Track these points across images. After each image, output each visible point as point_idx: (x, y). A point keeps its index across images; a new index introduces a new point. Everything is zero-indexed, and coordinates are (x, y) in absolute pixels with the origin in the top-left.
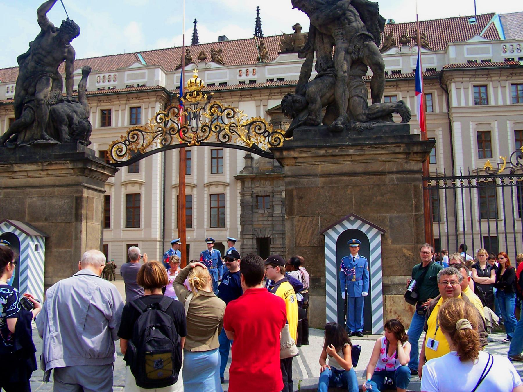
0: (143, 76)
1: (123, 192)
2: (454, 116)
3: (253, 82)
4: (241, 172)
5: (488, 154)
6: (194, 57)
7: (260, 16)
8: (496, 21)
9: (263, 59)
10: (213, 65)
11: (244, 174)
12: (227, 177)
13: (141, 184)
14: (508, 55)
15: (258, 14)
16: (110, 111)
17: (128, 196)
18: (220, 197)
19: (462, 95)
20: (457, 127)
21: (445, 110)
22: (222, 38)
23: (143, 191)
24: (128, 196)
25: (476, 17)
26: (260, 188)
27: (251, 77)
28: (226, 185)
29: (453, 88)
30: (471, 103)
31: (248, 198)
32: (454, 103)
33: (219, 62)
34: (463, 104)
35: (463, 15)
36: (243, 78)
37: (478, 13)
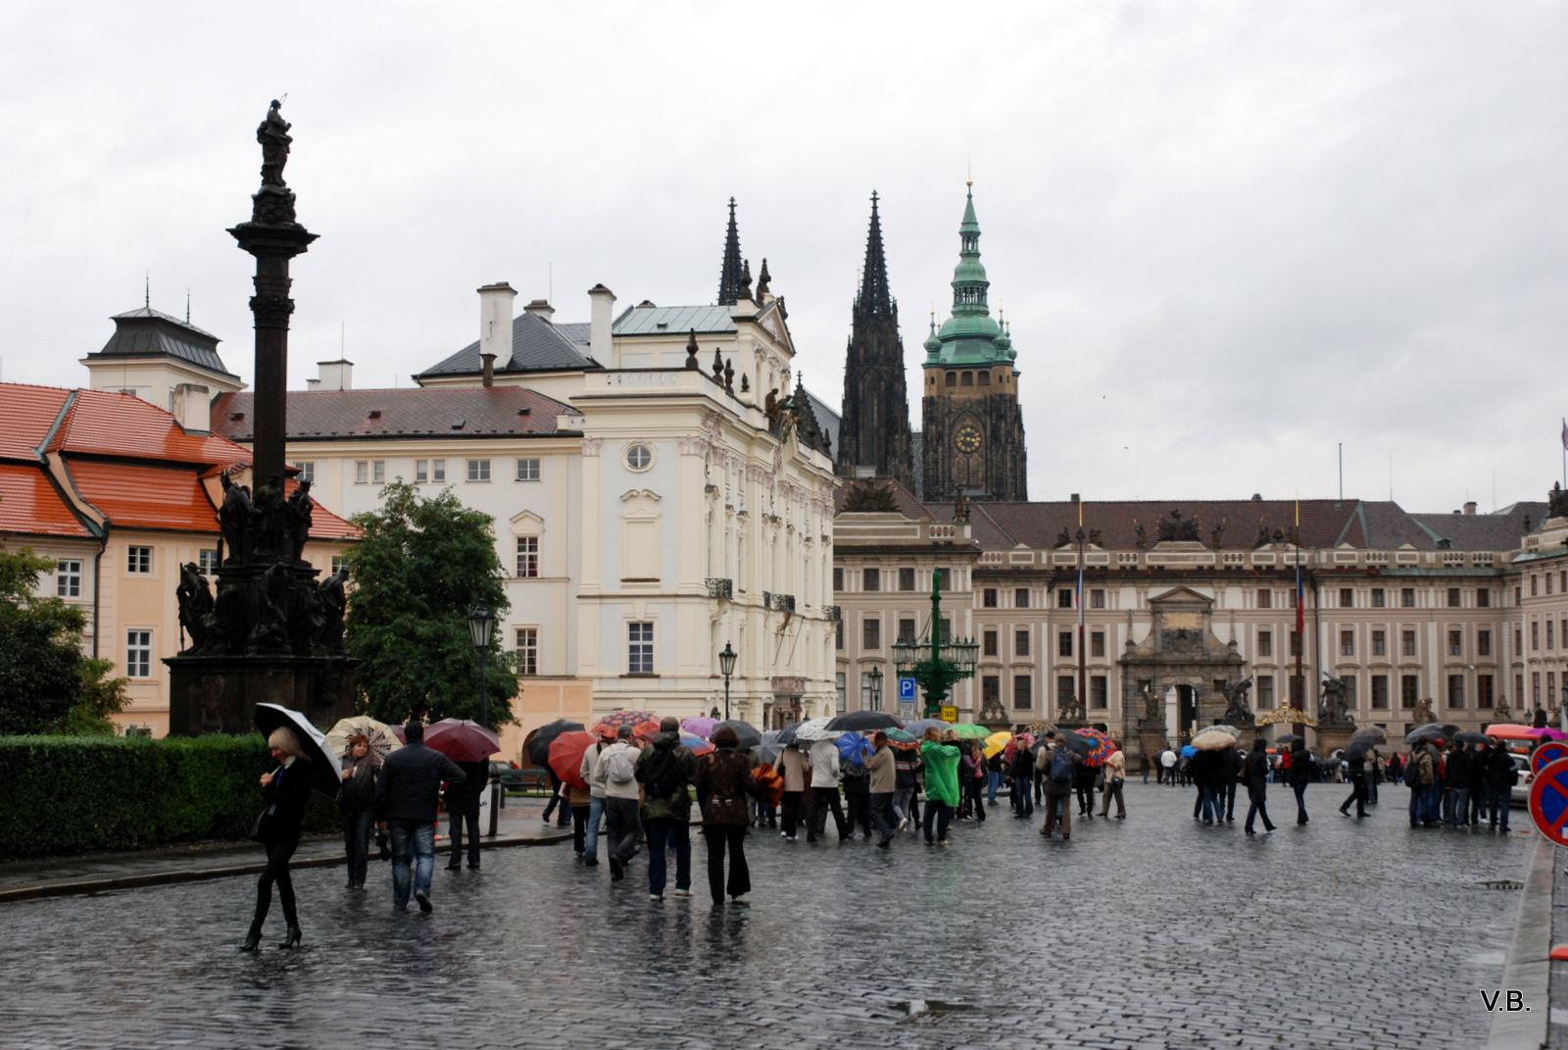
0: (1028, 558)
1: (1012, 673)
2: (1322, 616)
3: (1134, 568)
4: (1125, 655)
5: (1349, 651)
6: (1072, 536)
7: (880, 212)
8: (1360, 510)
9: (1142, 545)
10: (1093, 547)
11: (1129, 658)
12: (1108, 659)
13: (1030, 666)
14: (1371, 562)
15: (875, 208)
16: (994, 592)
17: (1017, 678)
18: (1103, 679)
19: (1329, 597)
20: (1324, 627)
21: (1313, 606)
22: (1075, 497)
23: (1033, 673)
24: (1017, 678)
25: (1341, 501)
26: (1144, 674)
27: (1131, 562)
28: (1107, 668)
29: (1322, 590)
30: (1338, 605)
31: (1131, 682)
32: (1323, 605)
33: (1100, 544)
34: (1331, 606)
35: (1329, 498)
36: (1124, 562)
37: (1344, 498)
